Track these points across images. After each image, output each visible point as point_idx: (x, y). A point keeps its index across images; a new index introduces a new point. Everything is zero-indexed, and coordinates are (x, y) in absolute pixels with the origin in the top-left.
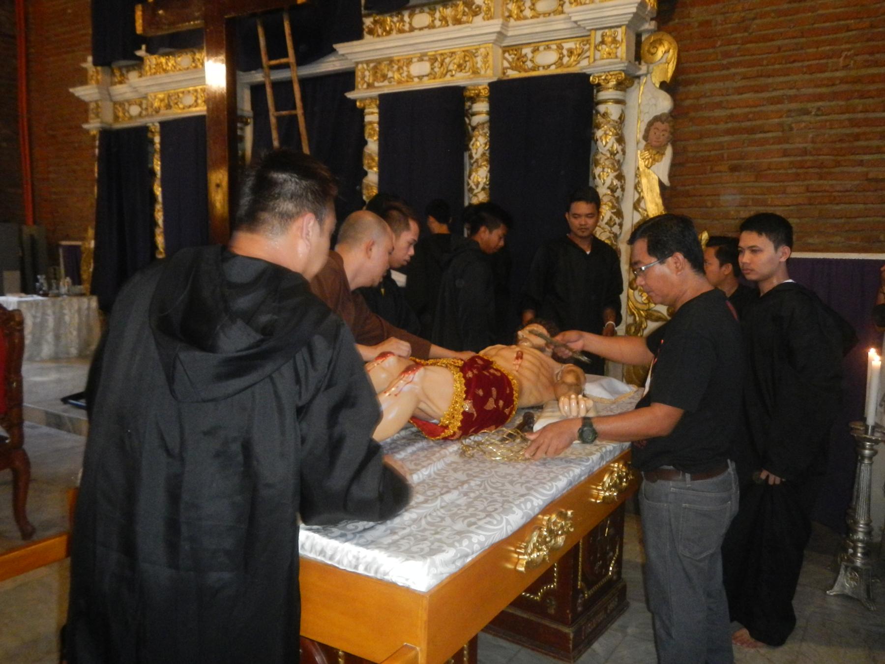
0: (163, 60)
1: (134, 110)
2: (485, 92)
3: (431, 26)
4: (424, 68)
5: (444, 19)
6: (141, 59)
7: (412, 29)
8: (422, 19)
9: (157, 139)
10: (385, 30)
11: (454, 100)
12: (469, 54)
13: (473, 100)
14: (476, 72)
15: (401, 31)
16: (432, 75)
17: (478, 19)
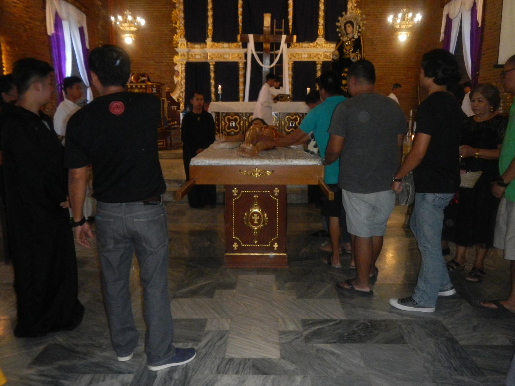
0: (216, 44)
1: (198, 57)
2: (322, 63)
3: (307, 47)
4: (306, 56)
5: (310, 46)
6: (205, 43)
7: (302, 47)
8: (305, 45)
9: (212, 67)
10: (294, 46)
11: (314, 64)
12: (317, 54)
13: (317, 64)
14: (319, 58)
15: (300, 47)
16: (308, 58)
17: (319, 47)
